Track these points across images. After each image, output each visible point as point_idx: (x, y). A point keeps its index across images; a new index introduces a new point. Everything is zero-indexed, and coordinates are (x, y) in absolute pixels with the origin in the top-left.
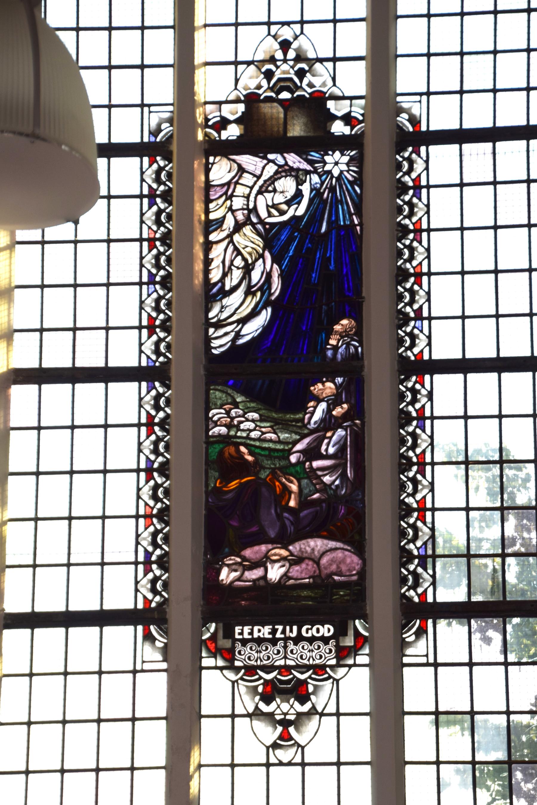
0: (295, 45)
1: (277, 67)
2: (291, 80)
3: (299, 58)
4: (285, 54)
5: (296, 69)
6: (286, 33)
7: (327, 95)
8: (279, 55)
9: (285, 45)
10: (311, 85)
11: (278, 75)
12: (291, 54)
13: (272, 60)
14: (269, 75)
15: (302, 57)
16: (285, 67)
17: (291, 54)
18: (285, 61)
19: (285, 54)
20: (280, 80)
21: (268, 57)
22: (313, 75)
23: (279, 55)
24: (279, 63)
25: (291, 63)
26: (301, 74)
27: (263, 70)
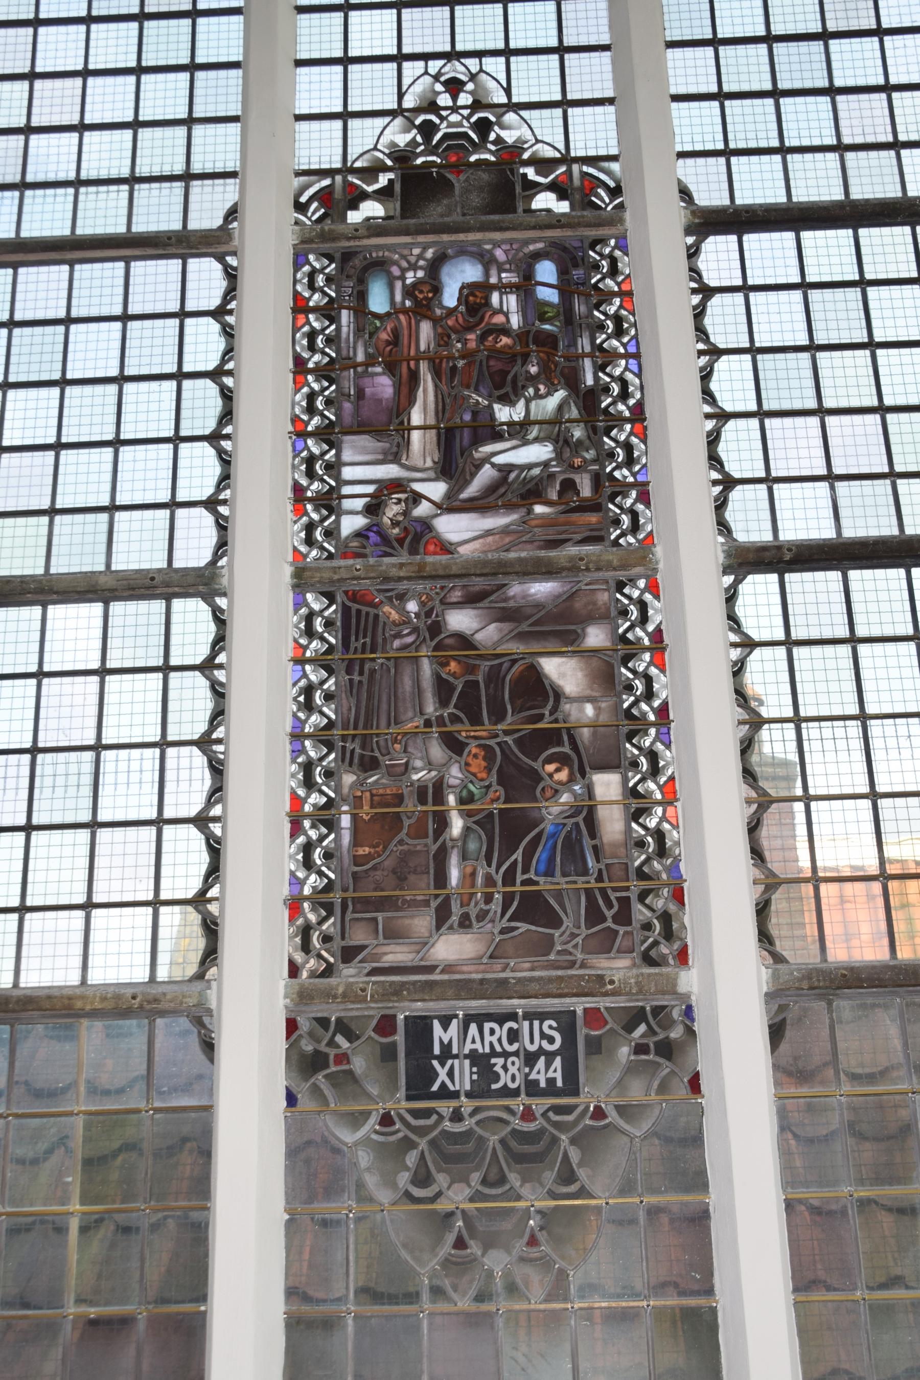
0: (470, 86)
1: (442, 118)
2: (465, 135)
3: (477, 105)
4: (455, 98)
5: (473, 120)
6: (456, 70)
7: (526, 156)
8: (444, 100)
9: (454, 86)
10: (499, 140)
11: (444, 129)
12: (465, 99)
13: (432, 107)
14: (427, 129)
15: (484, 101)
16: (454, 118)
17: (465, 99)
18: (454, 109)
19: (455, 98)
20: (446, 136)
21: (425, 105)
22: (502, 127)
23: (444, 100)
24: (444, 113)
25: (465, 112)
26: (483, 127)
27: (417, 122)
